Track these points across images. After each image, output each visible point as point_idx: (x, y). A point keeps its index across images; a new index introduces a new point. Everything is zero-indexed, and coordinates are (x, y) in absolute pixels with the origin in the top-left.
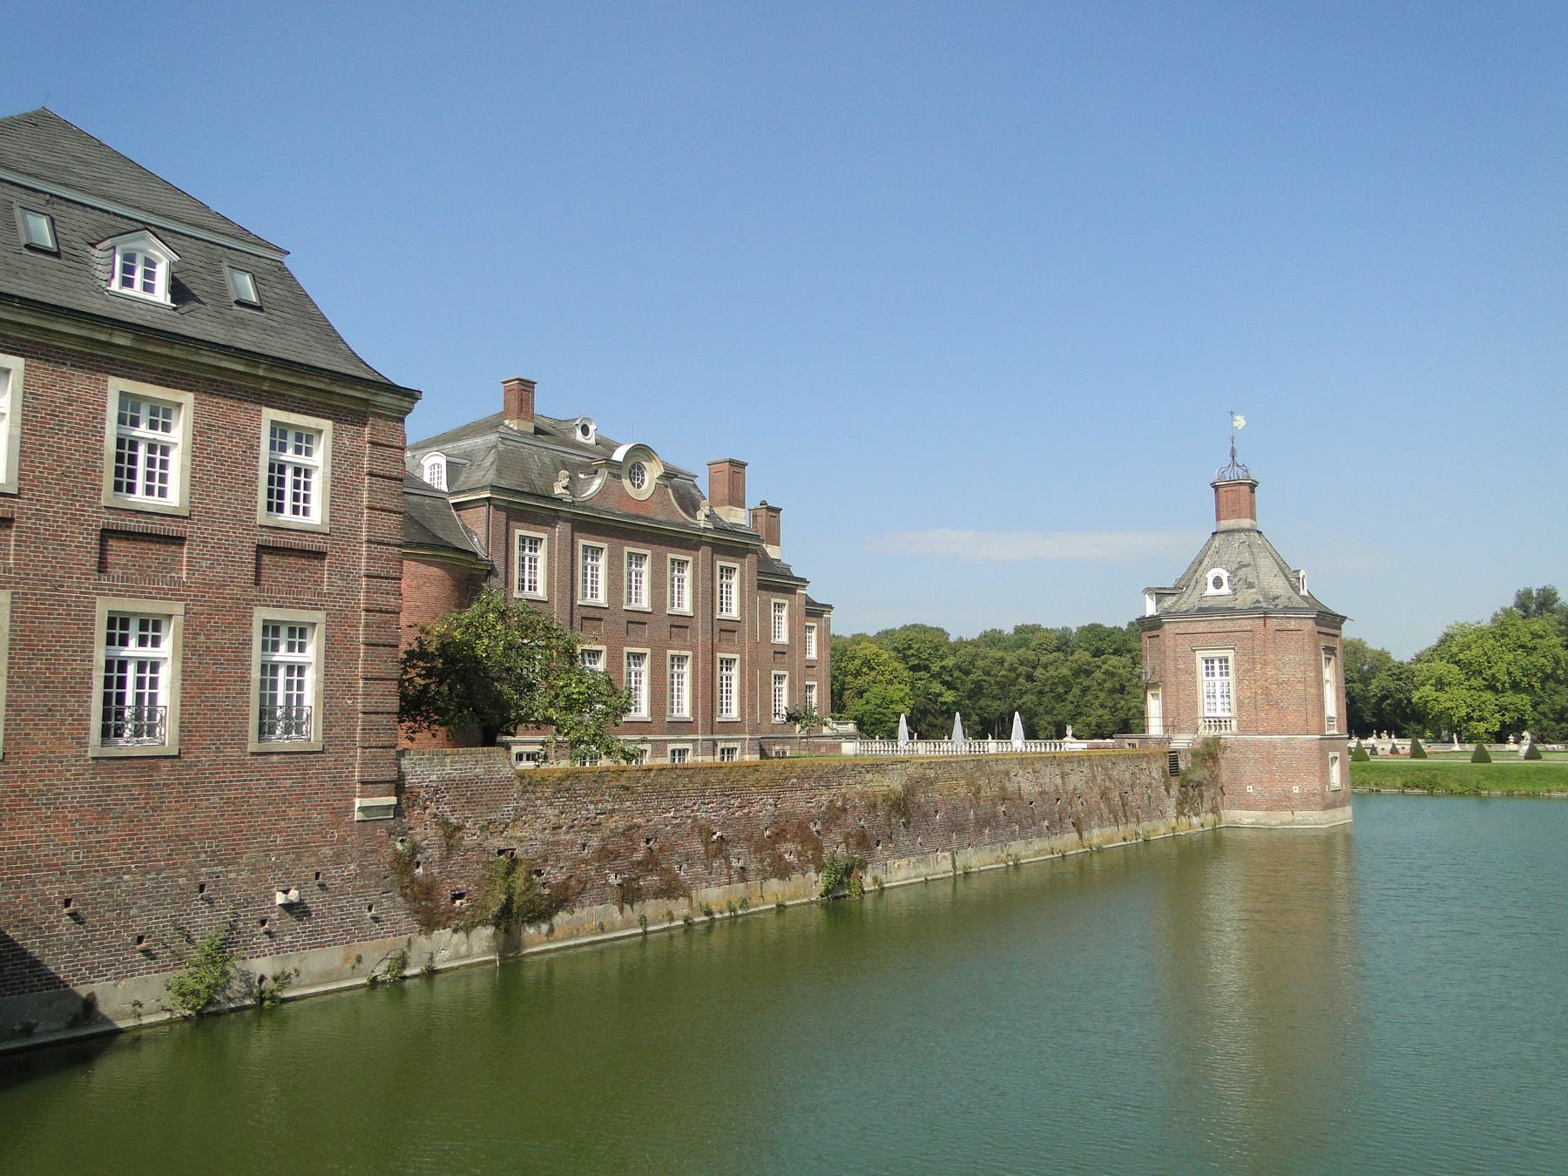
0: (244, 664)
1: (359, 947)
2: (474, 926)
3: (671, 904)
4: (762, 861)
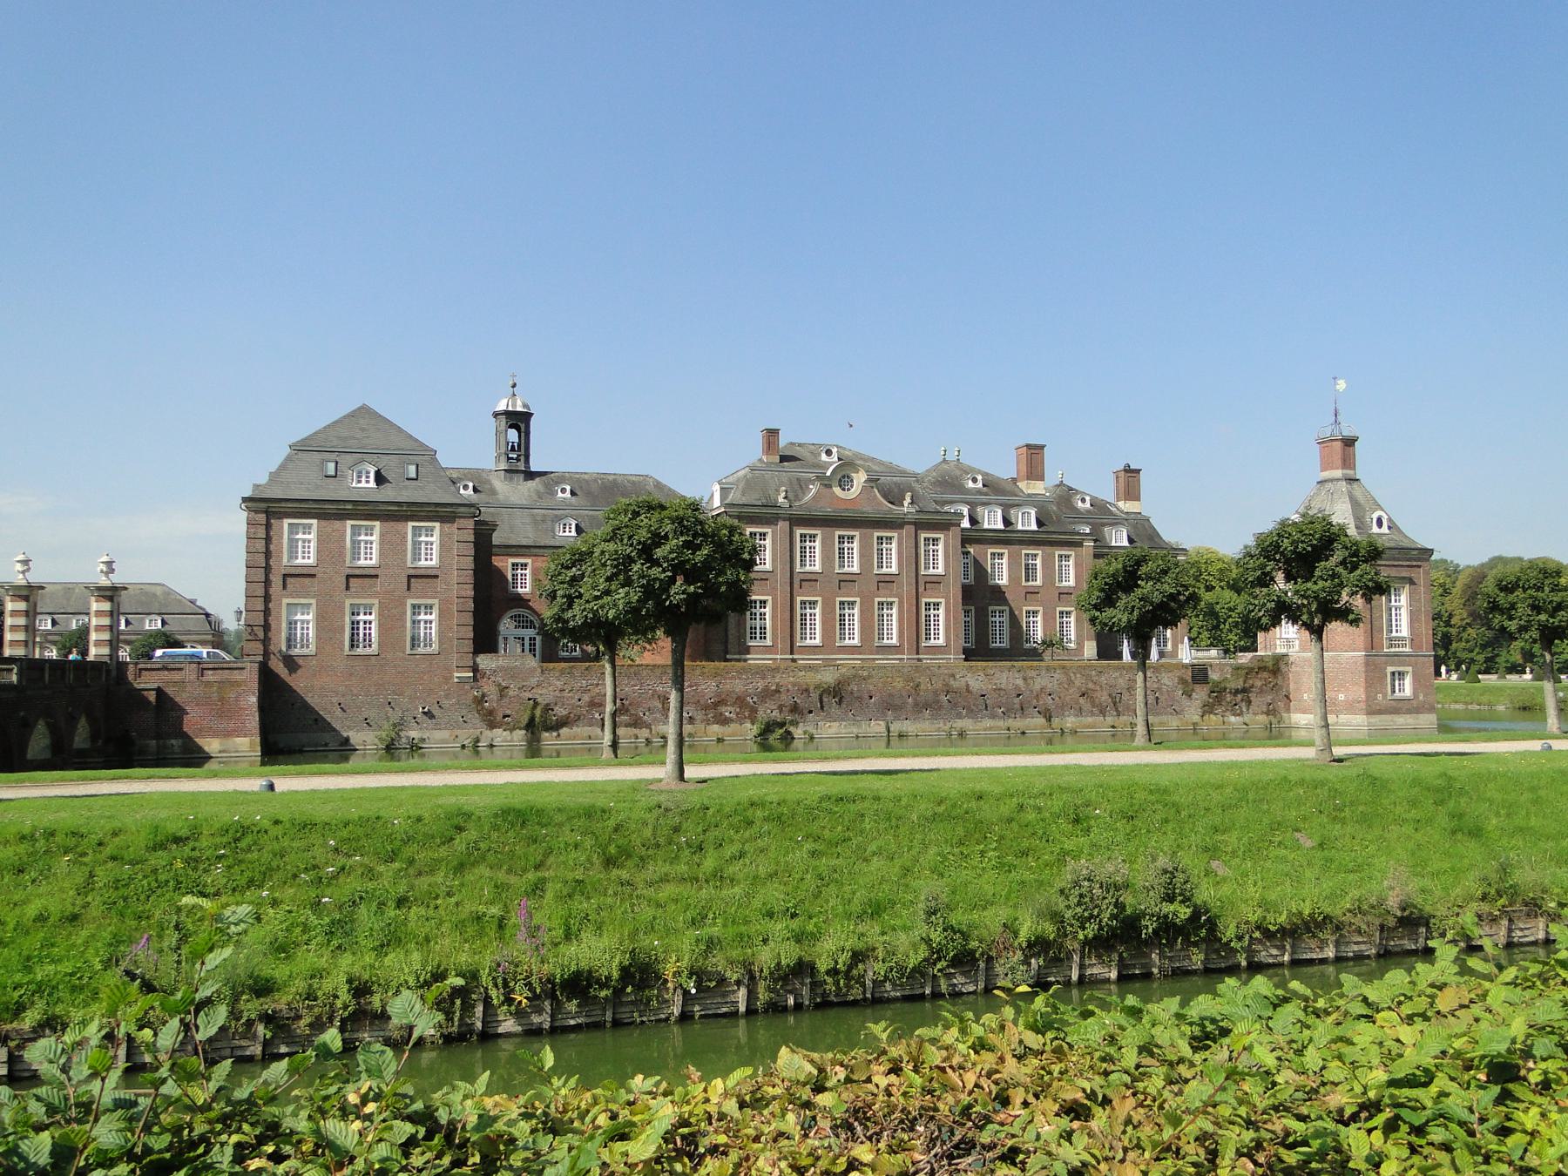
1: (458, 732)
3: (637, 731)
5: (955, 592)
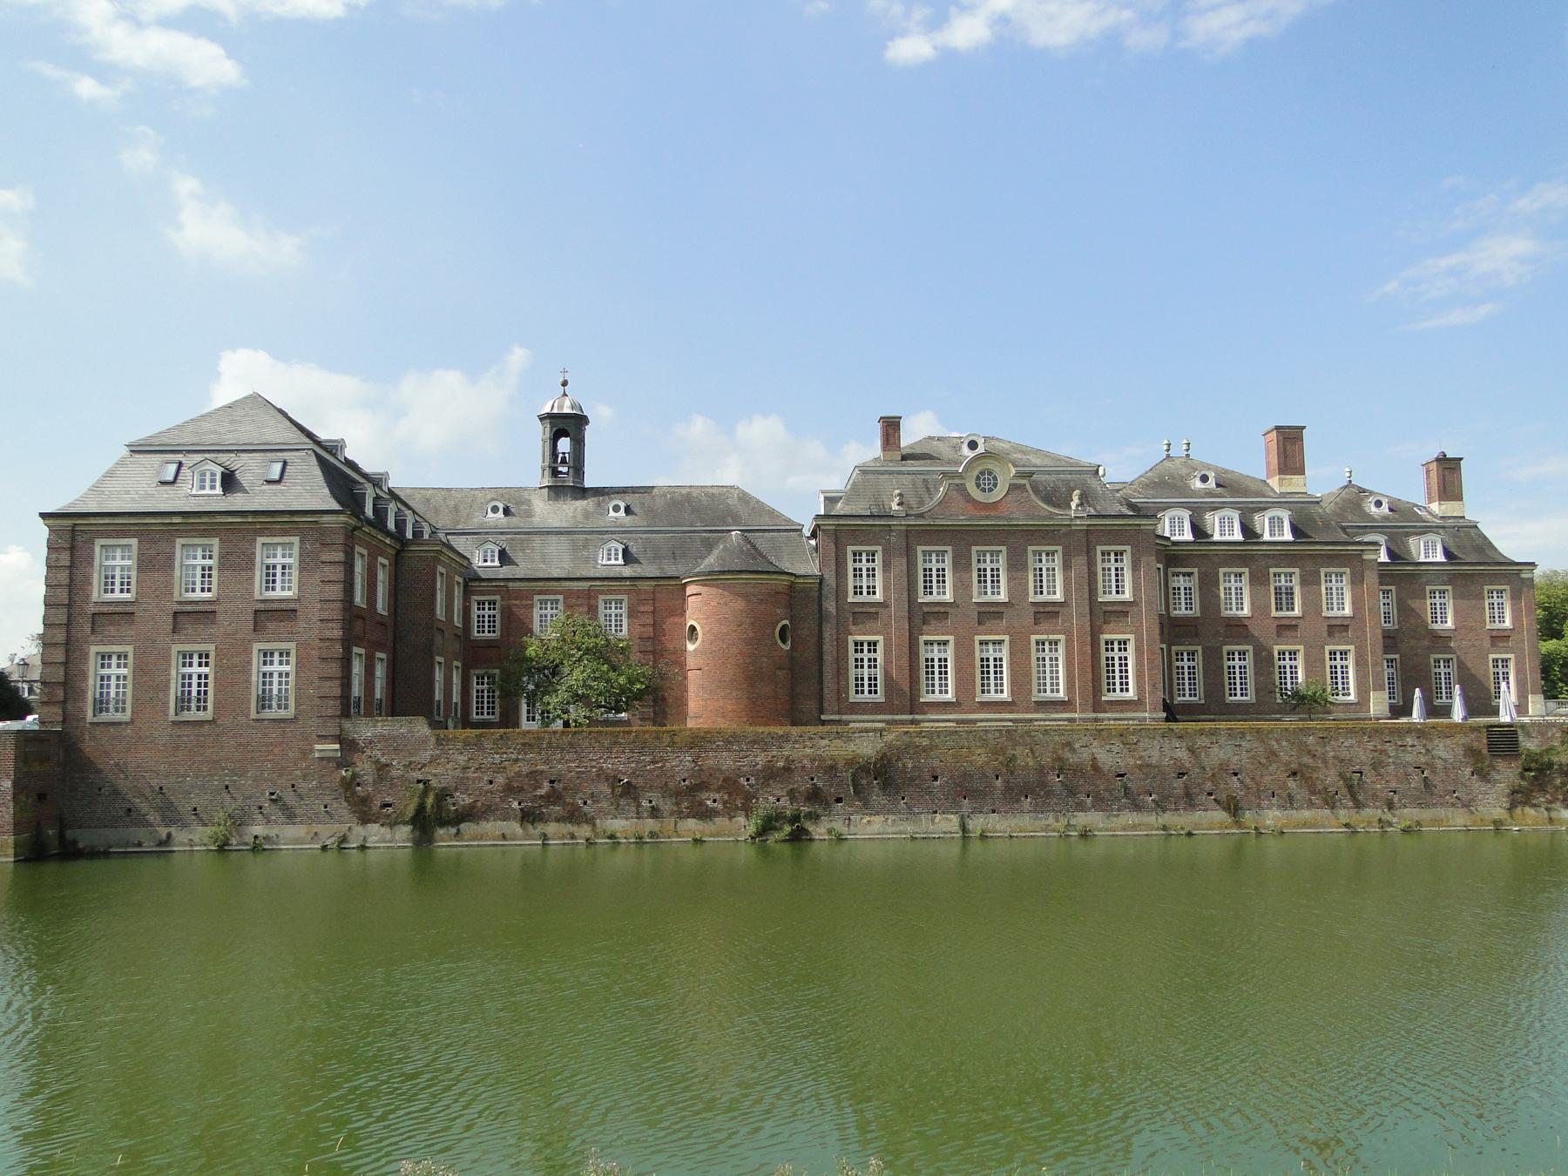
0: (248, 673)
2: (396, 823)
4: (677, 804)
5: (1148, 622)
